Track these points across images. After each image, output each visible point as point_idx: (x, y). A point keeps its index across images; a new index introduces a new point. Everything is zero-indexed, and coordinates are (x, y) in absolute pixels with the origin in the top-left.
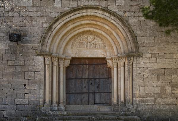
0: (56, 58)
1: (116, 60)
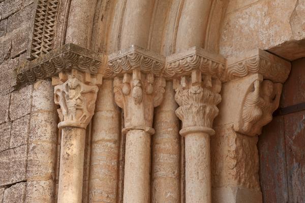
0: (130, 74)
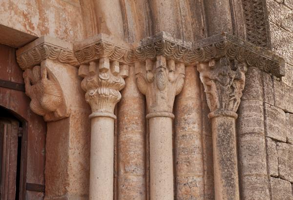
1: (117, 68)
